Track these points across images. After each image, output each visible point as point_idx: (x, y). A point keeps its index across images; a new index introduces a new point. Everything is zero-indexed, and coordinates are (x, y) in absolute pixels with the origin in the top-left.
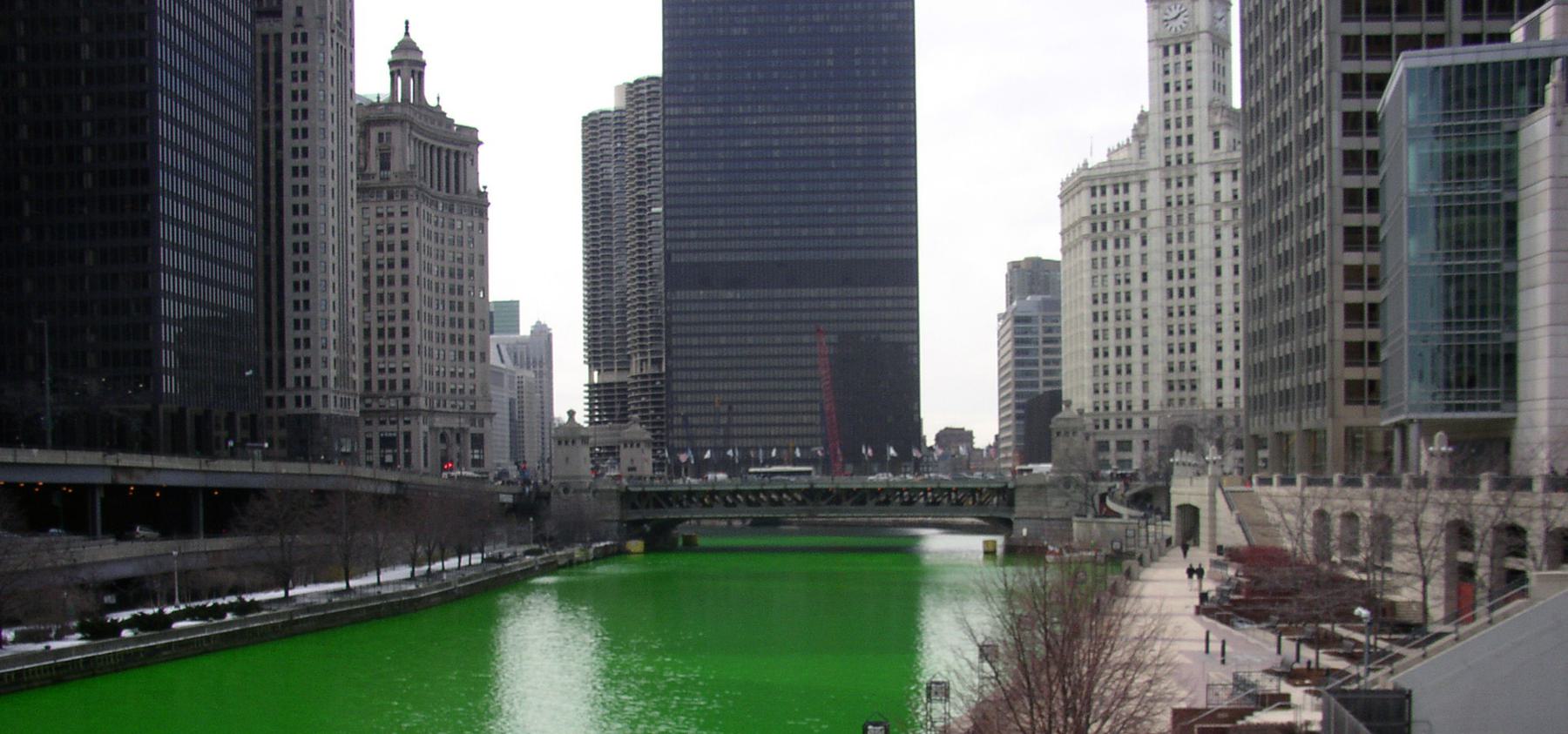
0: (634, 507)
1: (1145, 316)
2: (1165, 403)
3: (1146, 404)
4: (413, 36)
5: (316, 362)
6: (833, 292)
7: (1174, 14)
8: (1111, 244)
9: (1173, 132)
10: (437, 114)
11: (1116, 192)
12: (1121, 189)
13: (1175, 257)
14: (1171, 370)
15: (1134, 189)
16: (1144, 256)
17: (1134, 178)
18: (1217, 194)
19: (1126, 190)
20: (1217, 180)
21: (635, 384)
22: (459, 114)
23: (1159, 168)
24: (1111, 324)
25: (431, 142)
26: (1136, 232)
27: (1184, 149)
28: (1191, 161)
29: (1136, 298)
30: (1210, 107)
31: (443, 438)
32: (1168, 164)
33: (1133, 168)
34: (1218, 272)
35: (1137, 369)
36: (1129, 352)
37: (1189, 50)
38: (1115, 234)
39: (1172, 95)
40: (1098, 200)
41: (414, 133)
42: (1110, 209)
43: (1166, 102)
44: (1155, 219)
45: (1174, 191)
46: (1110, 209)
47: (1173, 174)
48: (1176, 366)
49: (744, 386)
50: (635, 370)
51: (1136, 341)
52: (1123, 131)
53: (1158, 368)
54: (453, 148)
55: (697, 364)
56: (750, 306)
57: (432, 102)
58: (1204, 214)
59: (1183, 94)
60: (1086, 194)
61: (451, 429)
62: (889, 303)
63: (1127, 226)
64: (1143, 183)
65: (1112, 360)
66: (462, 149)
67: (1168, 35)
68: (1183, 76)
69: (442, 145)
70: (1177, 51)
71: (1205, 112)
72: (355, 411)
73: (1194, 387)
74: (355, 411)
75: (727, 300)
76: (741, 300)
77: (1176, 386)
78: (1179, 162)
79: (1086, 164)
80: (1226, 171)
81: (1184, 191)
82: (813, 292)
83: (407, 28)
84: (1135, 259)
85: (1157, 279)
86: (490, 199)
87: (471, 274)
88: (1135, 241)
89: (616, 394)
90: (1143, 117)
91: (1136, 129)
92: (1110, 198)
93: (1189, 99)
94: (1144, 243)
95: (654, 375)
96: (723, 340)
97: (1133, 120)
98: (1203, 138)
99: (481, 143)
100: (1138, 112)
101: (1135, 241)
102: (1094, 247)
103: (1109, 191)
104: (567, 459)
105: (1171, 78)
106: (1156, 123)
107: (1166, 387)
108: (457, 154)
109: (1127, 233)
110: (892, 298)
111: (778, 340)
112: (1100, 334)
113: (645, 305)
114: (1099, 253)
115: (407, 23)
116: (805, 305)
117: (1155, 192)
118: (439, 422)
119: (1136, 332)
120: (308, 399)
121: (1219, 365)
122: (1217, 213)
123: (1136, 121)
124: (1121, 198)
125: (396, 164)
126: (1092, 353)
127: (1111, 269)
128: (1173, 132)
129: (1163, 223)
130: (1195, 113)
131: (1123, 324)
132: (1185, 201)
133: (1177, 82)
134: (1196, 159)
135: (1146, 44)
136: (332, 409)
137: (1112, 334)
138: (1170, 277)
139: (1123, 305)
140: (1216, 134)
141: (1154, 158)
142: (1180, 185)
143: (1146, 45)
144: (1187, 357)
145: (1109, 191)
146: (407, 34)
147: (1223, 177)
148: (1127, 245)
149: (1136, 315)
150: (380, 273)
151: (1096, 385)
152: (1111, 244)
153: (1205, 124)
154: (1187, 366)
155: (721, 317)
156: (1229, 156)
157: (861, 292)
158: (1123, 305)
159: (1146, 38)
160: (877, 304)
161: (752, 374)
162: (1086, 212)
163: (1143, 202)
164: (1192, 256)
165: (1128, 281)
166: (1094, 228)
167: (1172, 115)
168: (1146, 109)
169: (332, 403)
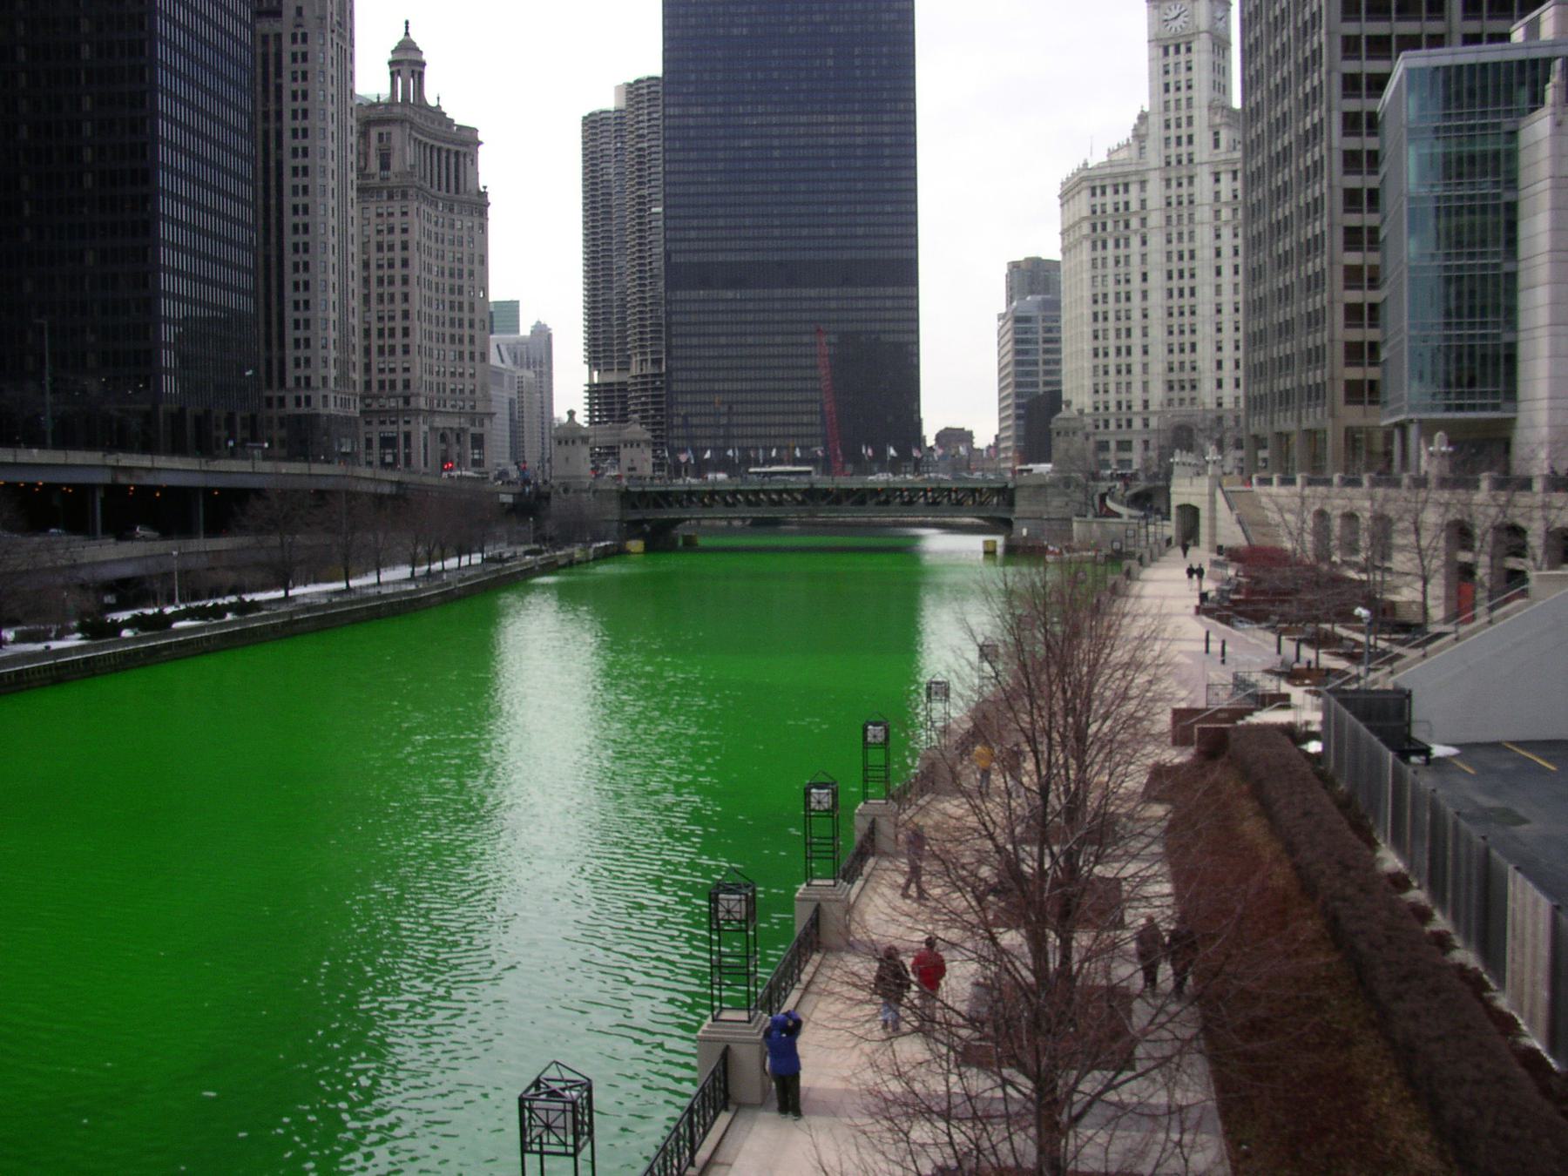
0: (634, 506)
1: (1145, 316)
2: (1165, 402)
3: (1146, 404)
4: (413, 36)
5: (316, 362)
6: (833, 292)
7: (1174, 14)
8: (1111, 244)
9: (1173, 132)
10: (437, 114)
11: (1116, 192)
12: (1121, 189)
13: (1175, 257)
14: (1171, 370)
15: (1134, 189)
16: (1144, 256)
17: (1134, 178)
18: (1217, 194)
19: (1126, 190)
20: (1217, 180)
21: (636, 384)
22: (459, 114)
23: (1159, 168)
24: (1111, 324)
25: (431, 142)
26: (1136, 232)
27: (1184, 149)
28: (1191, 161)
29: (1136, 298)
30: (1210, 108)
31: (443, 438)
32: (1168, 164)
33: (1133, 168)
34: (1218, 272)
35: (1137, 369)
36: (1129, 352)
37: (1189, 50)
38: (1116, 234)
39: (1172, 95)
40: (1098, 200)
41: (414, 134)
42: (1110, 209)
43: (1167, 102)
44: (1155, 219)
45: (1174, 191)
46: (1110, 209)
47: (1173, 175)
48: (1176, 366)
49: (745, 386)
50: (635, 370)
51: (1136, 340)
52: (1122, 131)
53: (1158, 368)
54: (453, 148)
55: (698, 364)
56: (750, 306)
57: (432, 102)
58: (1204, 214)
59: (1183, 94)
60: (1086, 194)
61: (451, 429)
62: (889, 303)
63: (1127, 226)
64: (1143, 183)
65: (1112, 360)
66: (462, 149)
68: (1183, 76)
69: (442, 145)
70: (1177, 51)
71: (1205, 112)
72: (355, 411)
73: (1194, 387)
74: (355, 411)
75: (727, 300)
76: (741, 300)
77: (1176, 387)
78: (1179, 162)
79: (1086, 164)
80: (1226, 171)
81: (1184, 191)
82: (813, 293)
83: (407, 28)
84: (1135, 260)
85: (1157, 279)
86: (490, 198)
87: (471, 274)
88: (1135, 242)
89: (616, 394)
90: (1143, 117)
91: (1136, 129)
92: (1110, 198)
93: (1189, 99)
94: (1144, 243)
95: (654, 375)
96: (723, 340)
97: (1133, 120)
98: (1203, 138)
99: (480, 143)
100: (1138, 112)
101: (1135, 242)
102: (1094, 247)
103: (1109, 191)
104: (567, 459)
105: (1171, 79)
106: (1156, 123)
107: (1166, 387)
108: (457, 153)
109: (1127, 233)
110: (893, 298)
111: (778, 339)
112: (1100, 334)
113: (645, 305)
114: (1099, 253)
115: (407, 23)
116: (805, 305)
117: (1155, 192)
118: (439, 422)
120: (308, 399)
121: (1219, 364)
122: (1217, 213)
123: (1136, 121)
124: (1121, 198)
125: (395, 164)
126: (1092, 353)
128: (1173, 132)
129: (1164, 223)
130: (1195, 113)
131: (1123, 325)
132: (1185, 201)
133: (1177, 82)
134: (1196, 159)
135: (1146, 44)
136: (332, 409)
137: (1112, 334)
138: (1170, 277)
139: (1123, 305)
140: (1216, 133)
141: (1154, 158)
142: (1180, 185)
143: (1146, 45)
144: (1187, 357)
145: (1109, 191)
146: (407, 34)
147: (1223, 177)
148: (1127, 245)
149: (1136, 315)
150: (380, 273)
151: (1096, 385)
152: (1111, 244)
153: (1205, 124)
154: (1187, 366)
155: (721, 317)
156: (1229, 156)
157: (861, 292)
158: (1123, 305)
159: (1146, 38)
160: (877, 304)
161: (751, 374)
162: (1086, 212)
163: (1143, 202)
164: (1192, 256)
165: (1128, 281)
166: (1094, 228)
167: (1172, 115)
168: (1147, 109)
169: (332, 403)
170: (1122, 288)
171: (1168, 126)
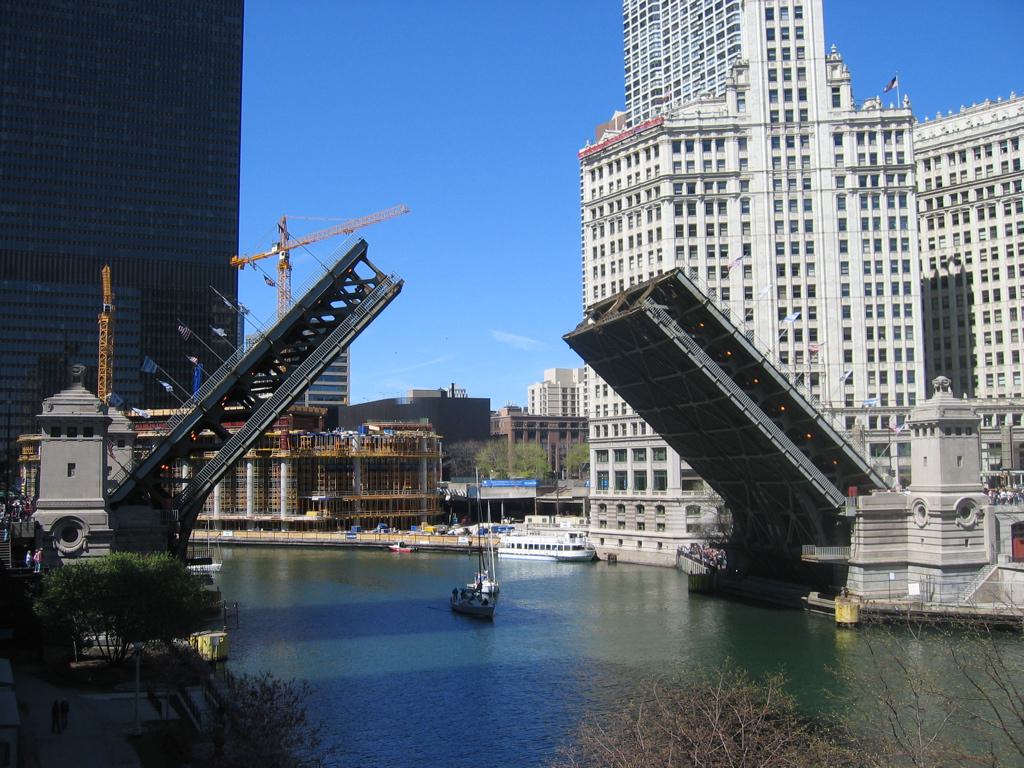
13: (786, 228)
15: (731, 146)
18: (839, 157)
27: (795, 105)
32: (774, 120)
33: (730, 122)
43: (771, 51)
44: (759, 183)
47: (782, 132)
58: (823, 180)
64: (742, 143)
84: (734, 228)
85: (763, 255)
88: (734, 207)
89: (188, 313)
94: (745, 211)
101: (734, 207)
104: (71, 466)
122: (840, 180)
130: (808, 64)
140: (836, 90)
145: (698, 147)
147: (846, 139)
153: (822, 80)
156: (853, 116)
171: (773, 79)
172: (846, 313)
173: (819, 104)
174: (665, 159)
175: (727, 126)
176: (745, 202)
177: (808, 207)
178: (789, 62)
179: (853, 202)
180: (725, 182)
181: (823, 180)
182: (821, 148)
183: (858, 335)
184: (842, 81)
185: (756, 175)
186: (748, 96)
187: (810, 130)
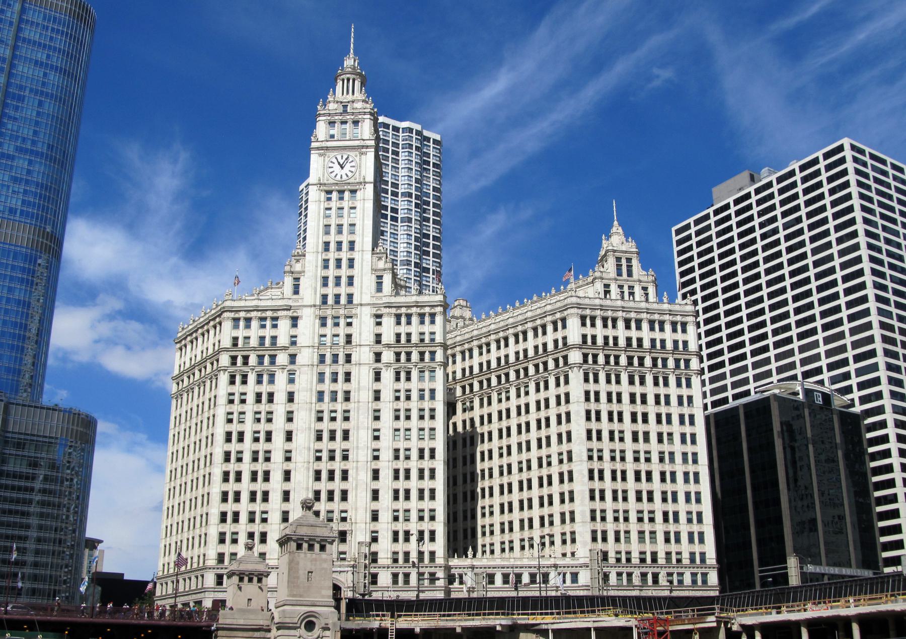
8: (252, 378)
15: (284, 325)
18: (378, 338)
20: (379, 324)
36: (265, 499)
38: (259, 369)
47: (329, 312)
58: (363, 355)
64: (295, 321)
67: (332, 181)
80: (389, 314)
94: (292, 381)
101: (281, 378)
102: (232, 382)
109: (273, 368)
119: (277, 476)
121: (375, 517)
122: (378, 357)
124: (268, 332)
127: (250, 407)
130: (356, 255)
134: (356, 300)
140: (380, 277)
147: (384, 320)
148: (272, 381)
149: (277, 456)
152: (252, 378)
153: (367, 268)
156: (393, 300)
162: (227, 343)
166: (234, 359)
170: (263, 427)
172: (376, 475)
173: (364, 289)
174: (227, 333)
175: (281, 306)
176: (292, 373)
177: (348, 377)
178: (341, 253)
179: (388, 376)
180: (276, 355)
181: (363, 355)
182: (363, 329)
183: (386, 496)
184: (385, 270)
185: (303, 349)
186: (302, 282)
187: (354, 311)
